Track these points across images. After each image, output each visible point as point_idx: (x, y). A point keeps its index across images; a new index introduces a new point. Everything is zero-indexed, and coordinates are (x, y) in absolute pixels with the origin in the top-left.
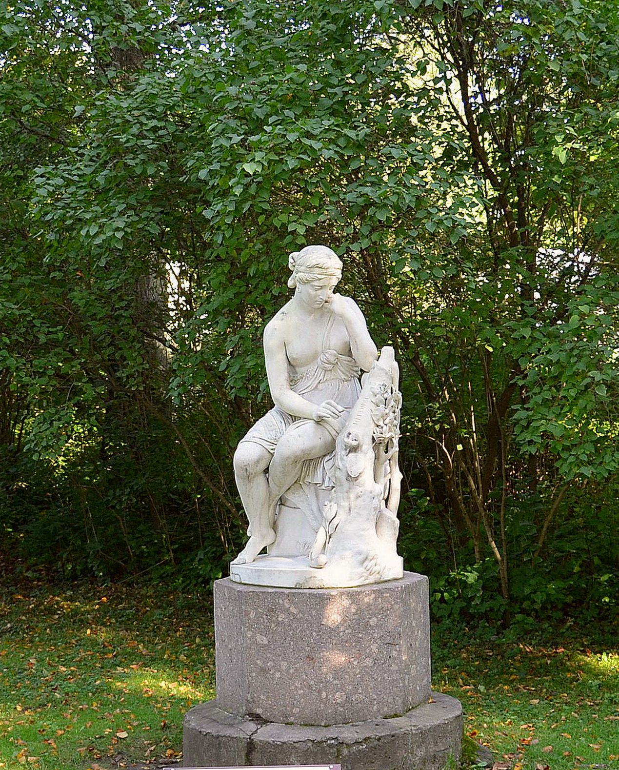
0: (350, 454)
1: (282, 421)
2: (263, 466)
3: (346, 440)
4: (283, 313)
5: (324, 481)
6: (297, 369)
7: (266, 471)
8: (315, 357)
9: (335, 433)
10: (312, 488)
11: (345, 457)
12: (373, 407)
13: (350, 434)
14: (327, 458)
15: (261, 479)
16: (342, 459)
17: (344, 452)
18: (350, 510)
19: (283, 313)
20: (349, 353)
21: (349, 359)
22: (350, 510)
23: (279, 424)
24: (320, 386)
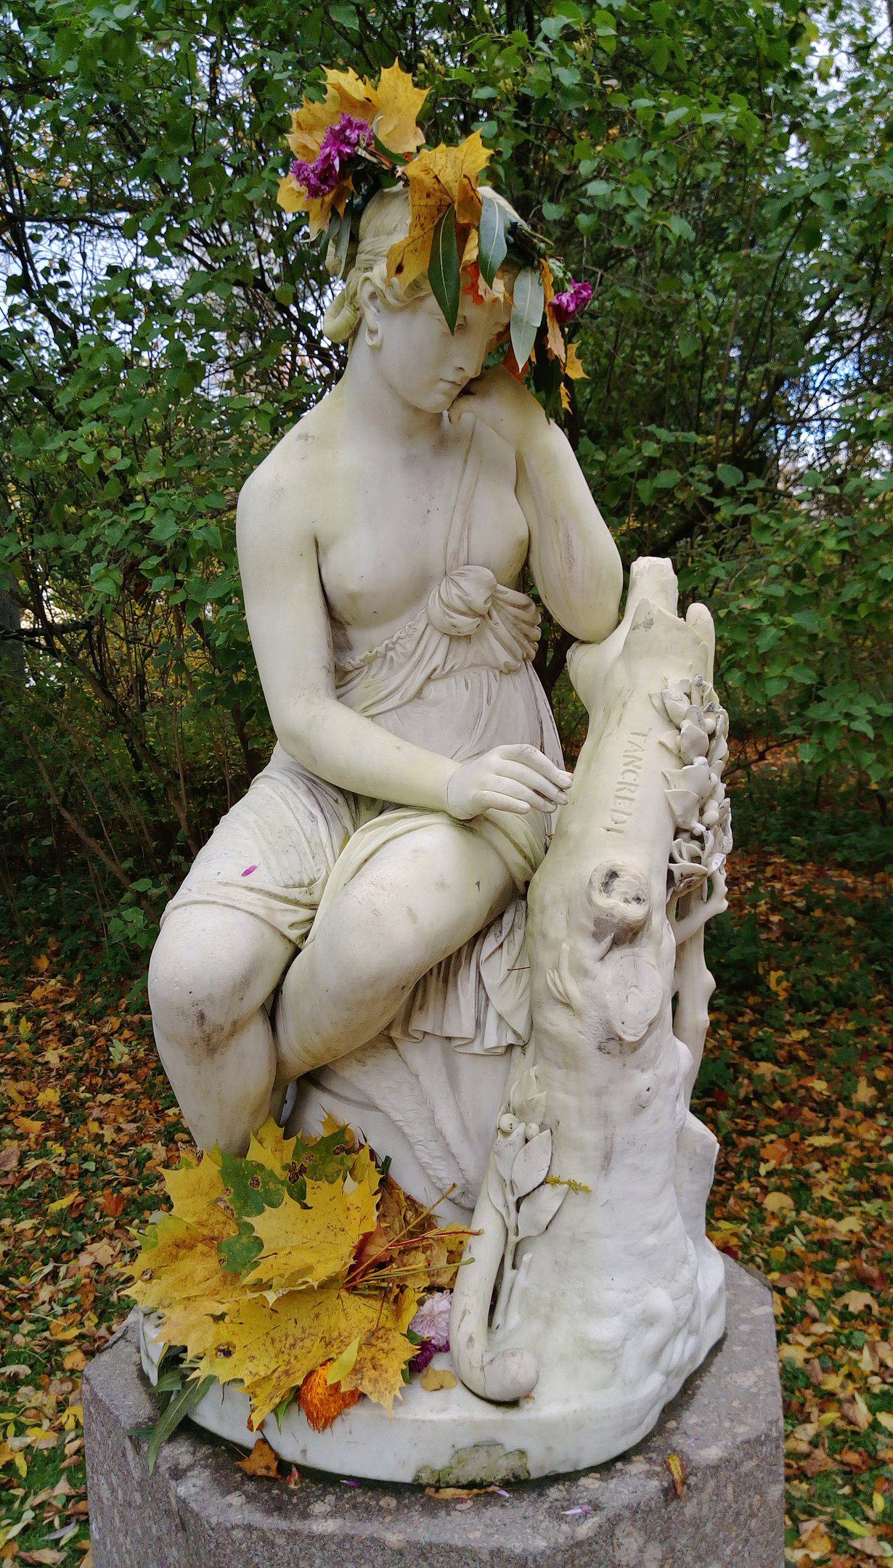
0: (617, 954)
1: (316, 812)
2: (260, 992)
3: (602, 900)
4: (305, 437)
5: (479, 1025)
6: (355, 634)
7: (271, 1010)
8: (418, 588)
9: (520, 859)
10: (435, 1047)
11: (595, 967)
12: (668, 765)
13: (613, 875)
14: (490, 944)
15: (258, 1029)
16: (581, 972)
17: (589, 950)
18: (608, 1157)
19: (305, 437)
20: (524, 580)
21: (521, 598)
22: (608, 1157)
23: (308, 826)
24: (432, 691)
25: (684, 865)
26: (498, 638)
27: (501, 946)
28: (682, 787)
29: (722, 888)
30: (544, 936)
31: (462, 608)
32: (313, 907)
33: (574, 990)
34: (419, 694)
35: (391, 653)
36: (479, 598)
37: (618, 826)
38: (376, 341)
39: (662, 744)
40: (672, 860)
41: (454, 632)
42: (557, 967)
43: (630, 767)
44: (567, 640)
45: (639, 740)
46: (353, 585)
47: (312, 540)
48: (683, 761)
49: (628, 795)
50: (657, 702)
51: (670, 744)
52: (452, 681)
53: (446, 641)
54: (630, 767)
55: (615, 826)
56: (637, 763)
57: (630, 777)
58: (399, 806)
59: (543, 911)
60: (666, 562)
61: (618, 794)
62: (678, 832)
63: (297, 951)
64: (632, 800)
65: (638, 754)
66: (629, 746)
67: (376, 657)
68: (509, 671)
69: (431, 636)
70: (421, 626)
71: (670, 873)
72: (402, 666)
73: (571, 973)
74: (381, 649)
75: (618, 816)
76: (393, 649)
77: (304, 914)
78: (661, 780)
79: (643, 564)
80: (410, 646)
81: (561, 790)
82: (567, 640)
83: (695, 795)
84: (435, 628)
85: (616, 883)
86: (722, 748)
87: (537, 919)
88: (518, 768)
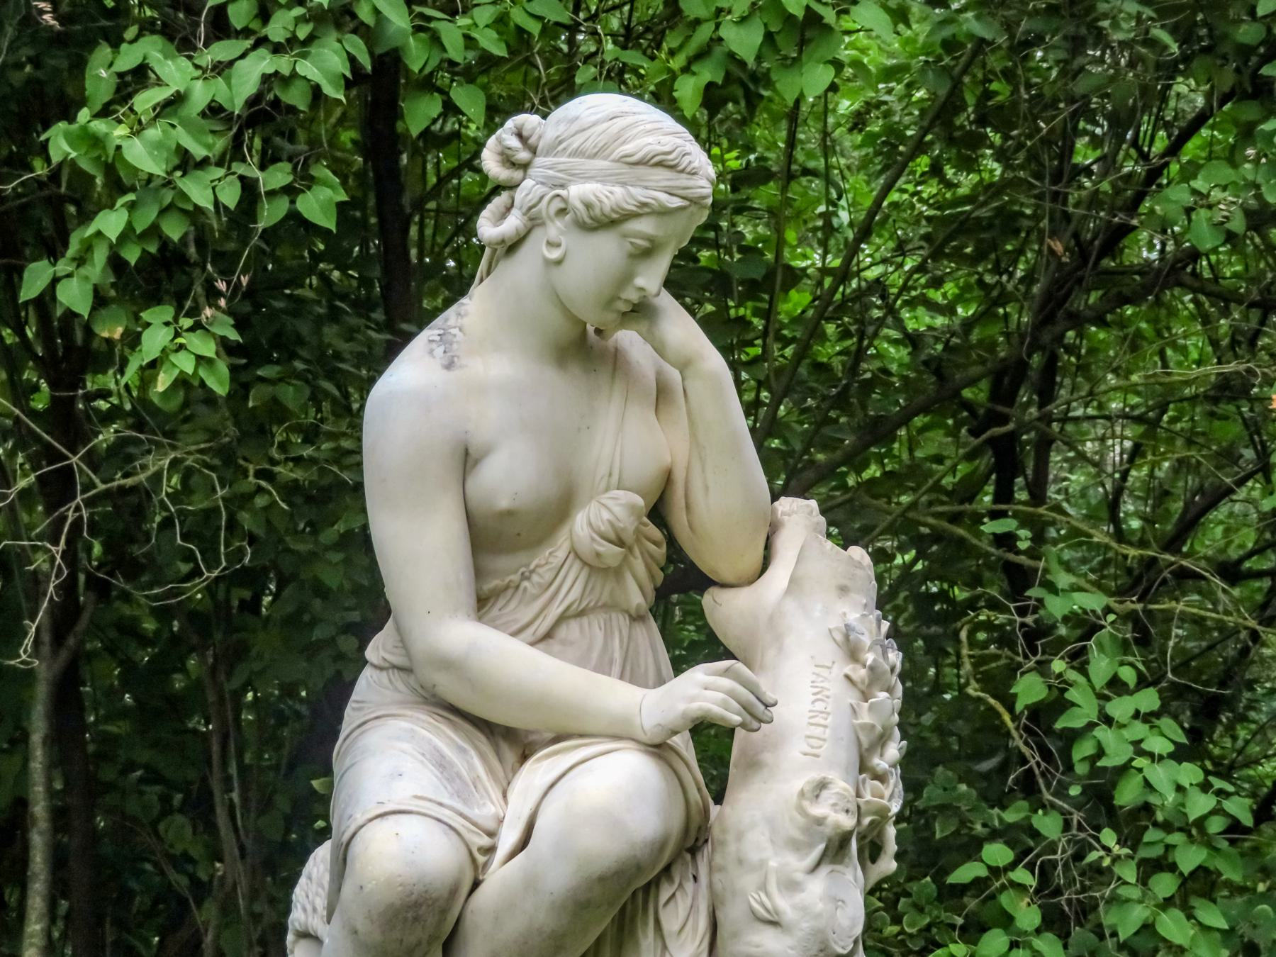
0: (825, 870)
1: (466, 746)
3: (818, 810)
12: (852, 697)
14: (665, 894)
17: (798, 864)
21: (656, 533)
25: (868, 797)
26: (635, 577)
27: (673, 895)
28: (866, 718)
29: (892, 847)
30: (740, 862)
31: (613, 536)
32: (491, 834)
33: (784, 905)
34: (548, 635)
35: (526, 584)
36: (628, 523)
37: (815, 751)
38: (555, 254)
39: (847, 677)
40: (858, 795)
41: (595, 563)
42: (763, 887)
43: (819, 696)
44: (704, 582)
45: (824, 672)
46: (504, 503)
47: (463, 452)
48: (865, 697)
49: (822, 722)
50: (839, 637)
51: (854, 677)
52: (585, 620)
53: (586, 570)
54: (819, 696)
55: (809, 750)
56: (826, 693)
57: (819, 706)
58: (557, 739)
59: (740, 837)
60: (813, 503)
61: (812, 721)
62: (863, 767)
63: (476, 884)
64: (825, 727)
65: (825, 685)
66: (814, 678)
67: (507, 587)
68: (636, 618)
69: (571, 567)
70: (561, 554)
71: (859, 807)
72: (536, 597)
73: (780, 890)
74: (515, 578)
75: (814, 742)
76: (528, 578)
77: (485, 841)
78: (849, 710)
79: (786, 504)
80: (548, 576)
81: (766, 706)
82: (704, 582)
83: (879, 728)
84: (577, 556)
85: (825, 794)
86: (900, 687)
87: (732, 848)
88: (726, 683)
